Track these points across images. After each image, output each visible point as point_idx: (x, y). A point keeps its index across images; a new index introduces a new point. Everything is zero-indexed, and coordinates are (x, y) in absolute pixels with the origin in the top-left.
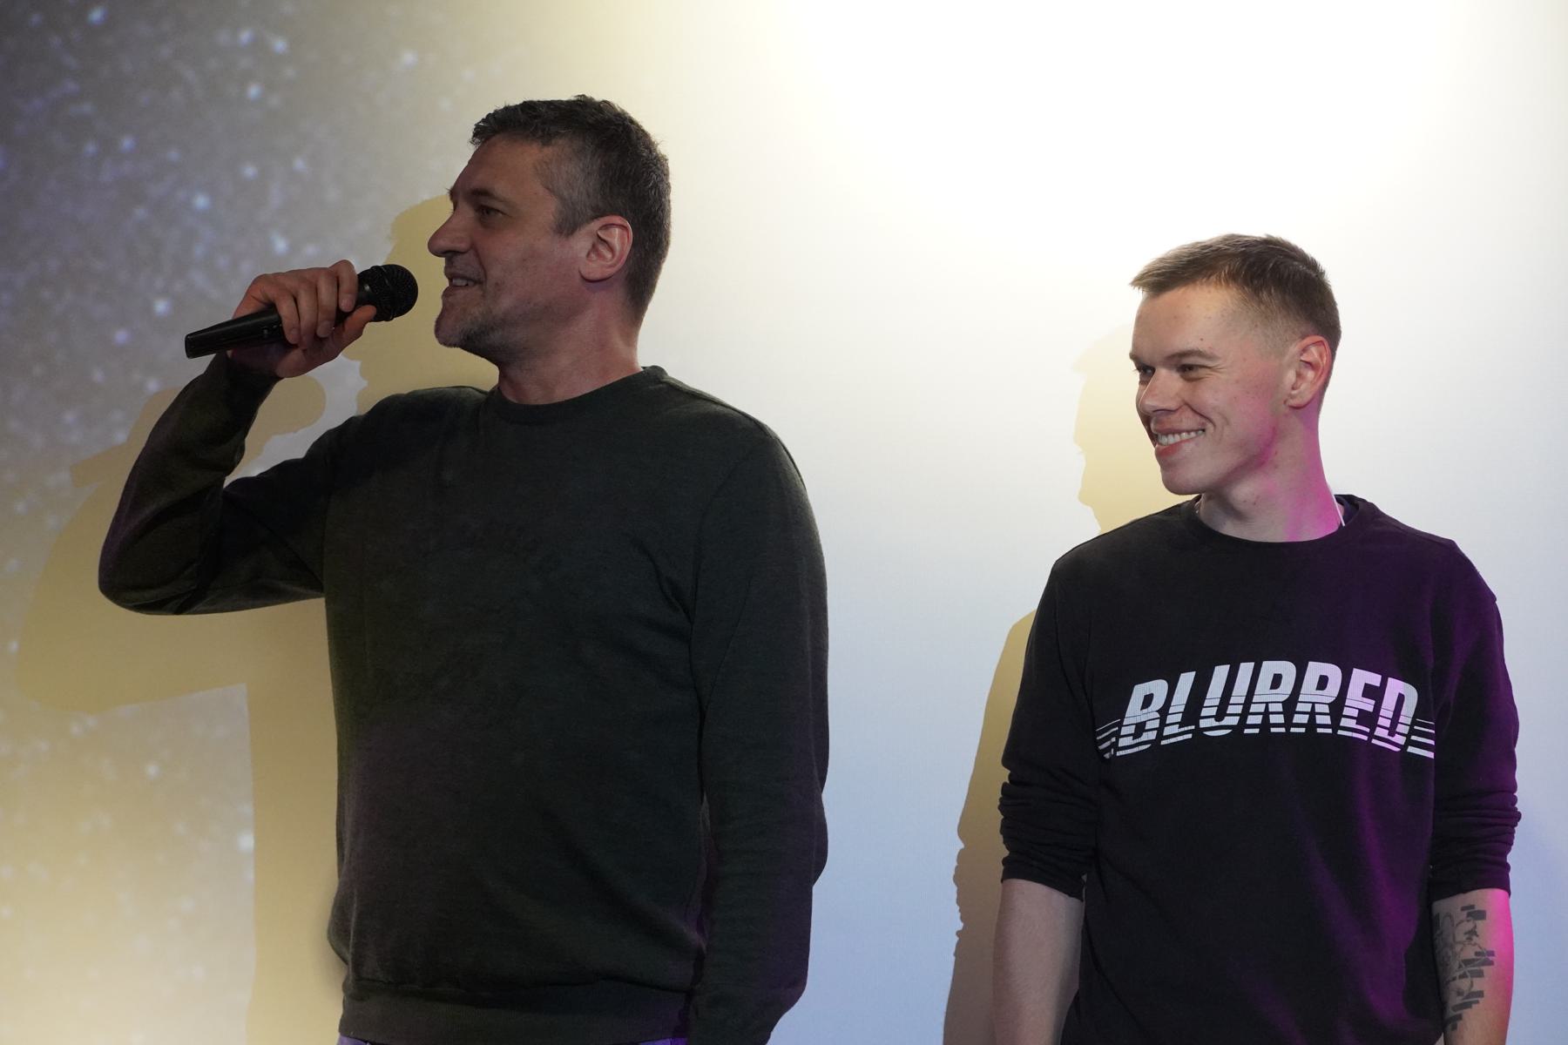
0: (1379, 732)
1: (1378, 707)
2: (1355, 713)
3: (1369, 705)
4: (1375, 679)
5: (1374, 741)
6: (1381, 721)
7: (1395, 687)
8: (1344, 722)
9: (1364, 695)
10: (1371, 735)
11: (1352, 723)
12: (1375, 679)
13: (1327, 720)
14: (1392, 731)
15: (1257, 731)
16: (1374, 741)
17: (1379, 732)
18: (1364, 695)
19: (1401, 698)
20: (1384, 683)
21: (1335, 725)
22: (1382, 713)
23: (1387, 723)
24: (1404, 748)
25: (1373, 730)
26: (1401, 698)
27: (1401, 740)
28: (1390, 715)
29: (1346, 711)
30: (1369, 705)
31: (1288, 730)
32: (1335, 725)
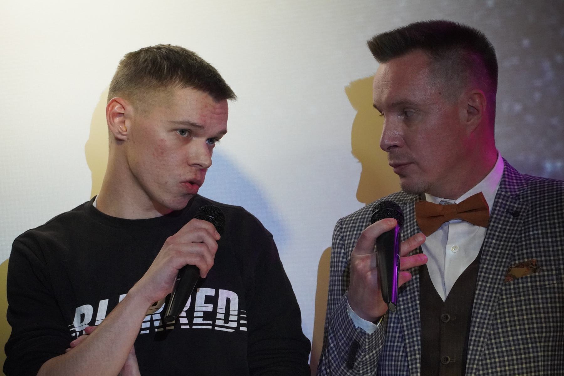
0: (218, 322)
1: (215, 308)
2: (201, 314)
3: (209, 308)
4: (211, 292)
5: (216, 328)
6: (218, 316)
7: (224, 294)
8: (196, 321)
9: (206, 302)
10: (214, 325)
11: (200, 321)
12: (211, 292)
13: (185, 321)
14: (226, 320)
15: (148, 332)
16: (216, 328)
17: (218, 322)
18: (206, 302)
19: (228, 301)
20: (217, 293)
21: (191, 323)
22: (219, 311)
23: (222, 316)
24: (237, 329)
25: (214, 322)
26: (228, 301)
27: (235, 325)
28: (224, 311)
29: (196, 314)
30: (209, 308)
31: (165, 329)
32: (191, 323)
